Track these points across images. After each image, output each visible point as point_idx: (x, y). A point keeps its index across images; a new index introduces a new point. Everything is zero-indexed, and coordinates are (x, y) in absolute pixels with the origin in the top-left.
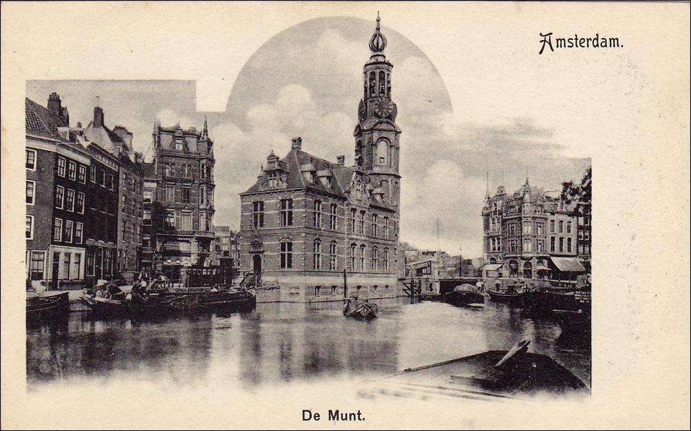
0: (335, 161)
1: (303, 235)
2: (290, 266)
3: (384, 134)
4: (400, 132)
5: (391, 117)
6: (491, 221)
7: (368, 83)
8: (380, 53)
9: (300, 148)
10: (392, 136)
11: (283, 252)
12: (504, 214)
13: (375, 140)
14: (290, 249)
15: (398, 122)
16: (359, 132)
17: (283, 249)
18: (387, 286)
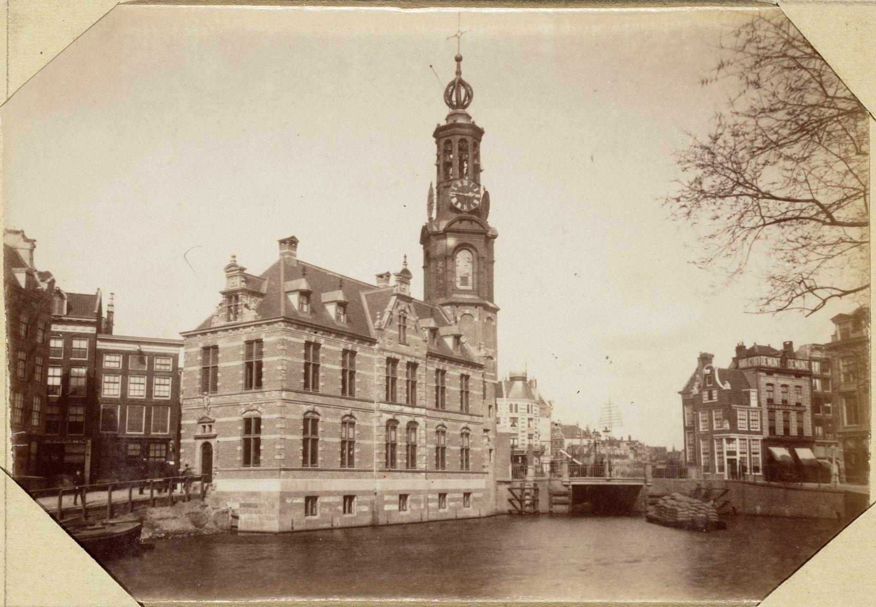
0: (373, 281)
1: (279, 403)
2: (257, 462)
3: (466, 239)
4: (495, 237)
5: (481, 211)
7: (441, 157)
9: (295, 256)
10: (479, 242)
11: (247, 436)
14: (258, 430)
15: (493, 220)
16: (427, 237)
17: (247, 430)
18: (467, 495)
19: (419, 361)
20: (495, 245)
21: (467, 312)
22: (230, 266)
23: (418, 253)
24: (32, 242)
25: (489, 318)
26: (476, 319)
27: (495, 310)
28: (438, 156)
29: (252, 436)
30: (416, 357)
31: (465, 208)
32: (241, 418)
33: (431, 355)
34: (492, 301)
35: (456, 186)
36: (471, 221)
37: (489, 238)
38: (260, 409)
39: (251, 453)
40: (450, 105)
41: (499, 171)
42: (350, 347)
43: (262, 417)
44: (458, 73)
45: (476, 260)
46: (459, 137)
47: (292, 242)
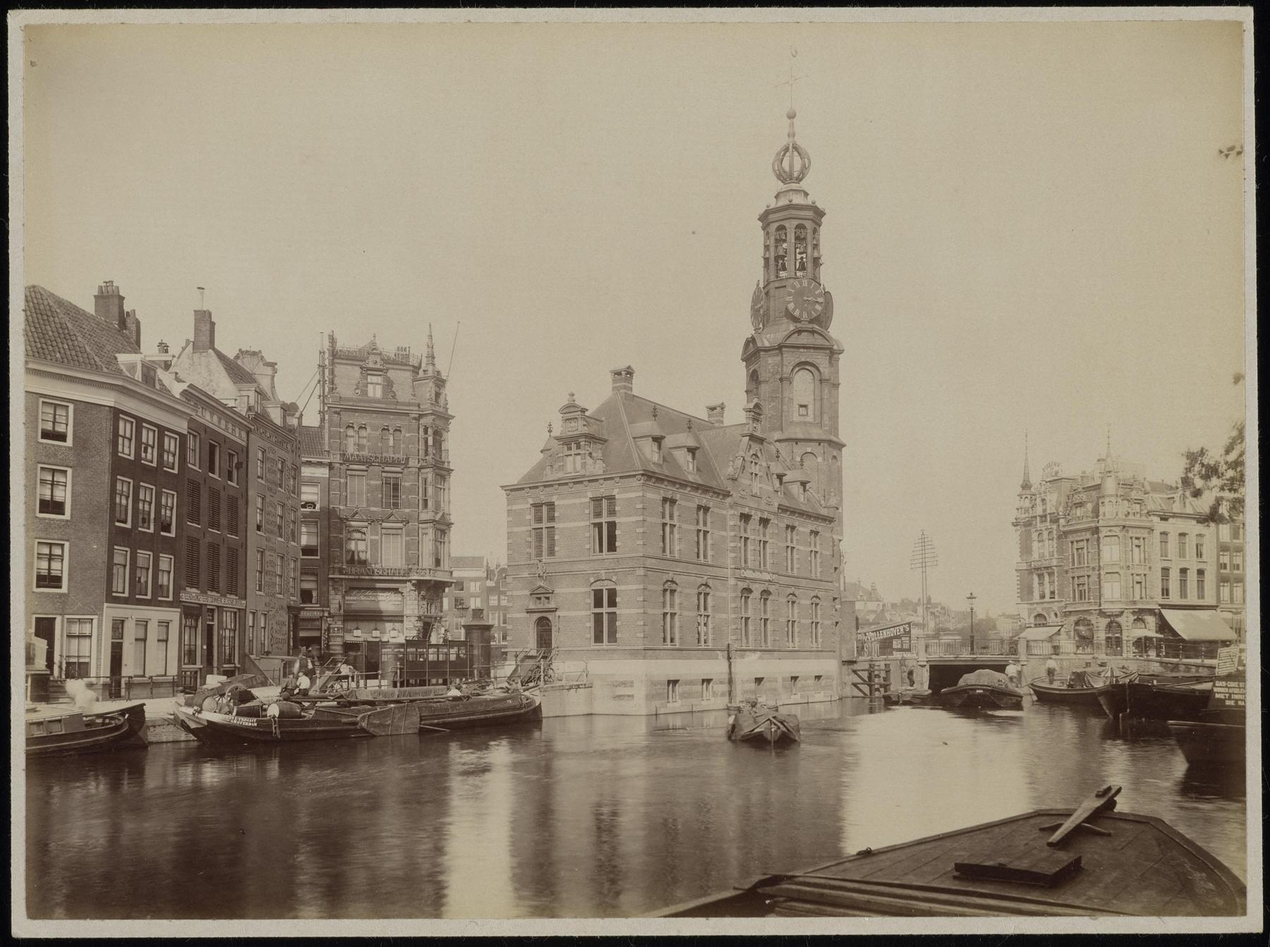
0: (703, 415)
1: (641, 572)
3: (804, 356)
4: (841, 352)
5: (822, 320)
6: (1035, 536)
7: (772, 249)
8: (794, 186)
10: (821, 360)
11: (598, 610)
12: (1062, 521)
13: (787, 370)
14: (612, 603)
15: (835, 330)
16: (752, 353)
17: (598, 603)
19: (772, 517)
20: (841, 363)
21: (809, 450)
22: (568, 407)
23: (740, 372)
24: (272, 365)
25: (835, 457)
26: (820, 459)
27: (840, 446)
28: (767, 247)
29: (605, 609)
30: (751, 508)
31: (805, 315)
32: (588, 589)
33: (783, 509)
34: (837, 435)
35: (794, 287)
36: (813, 332)
37: (833, 353)
38: (614, 579)
39: (604, 629)
40: (779, 177)
41: (841, 267)
42: (704, 503)
43: (618, 588)
44: (792, 135)
45: (818, 383)
46: (795, 222)
47: (625, 375)
